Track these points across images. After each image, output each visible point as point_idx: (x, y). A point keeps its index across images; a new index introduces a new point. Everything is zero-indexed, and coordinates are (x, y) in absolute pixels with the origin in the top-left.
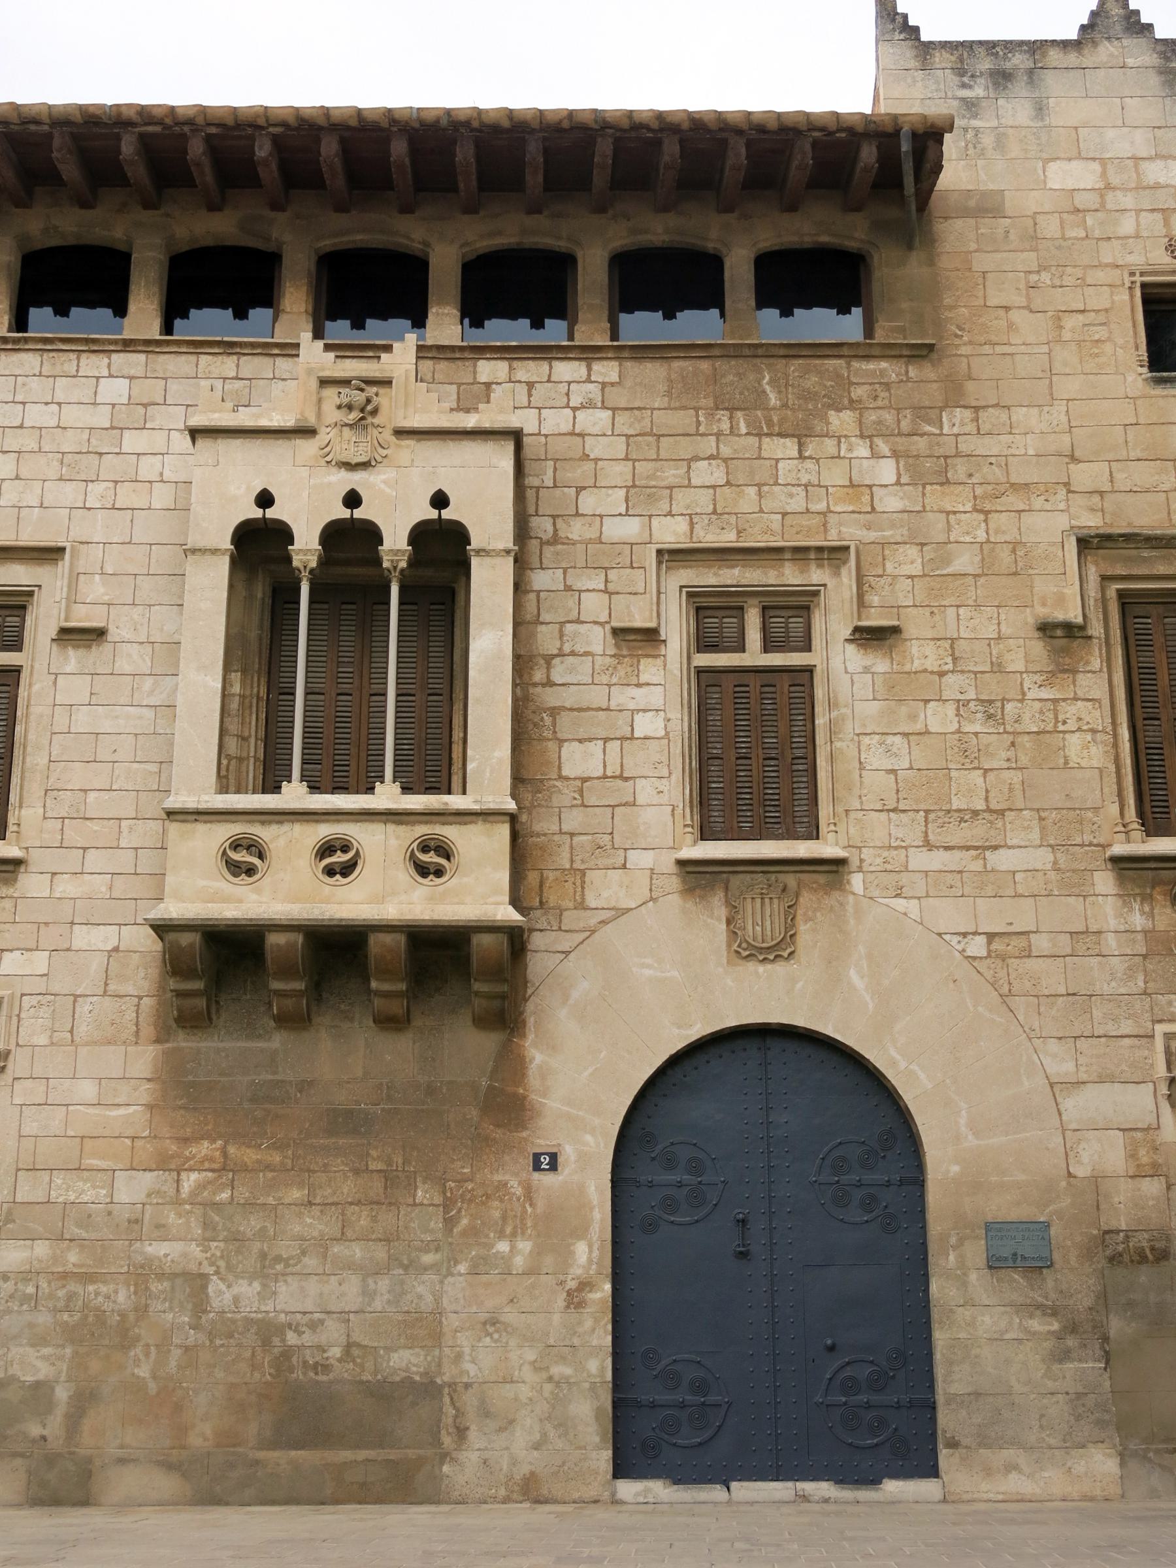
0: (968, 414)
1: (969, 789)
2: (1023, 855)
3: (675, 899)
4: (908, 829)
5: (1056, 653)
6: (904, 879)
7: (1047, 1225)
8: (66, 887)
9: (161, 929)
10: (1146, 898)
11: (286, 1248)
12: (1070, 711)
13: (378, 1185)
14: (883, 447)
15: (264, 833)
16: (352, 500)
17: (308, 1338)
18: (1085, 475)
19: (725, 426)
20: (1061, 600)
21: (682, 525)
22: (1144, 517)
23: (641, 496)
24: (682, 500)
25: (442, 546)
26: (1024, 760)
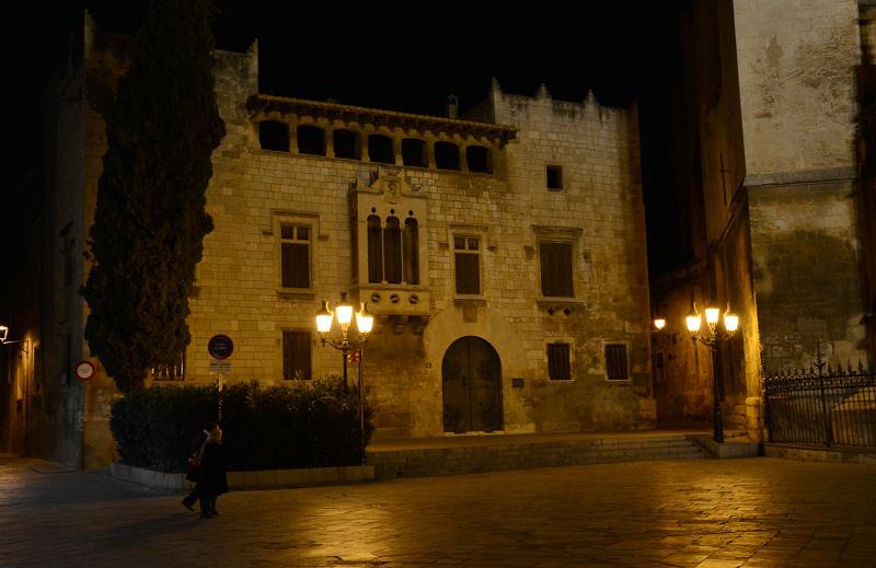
1: (510, 285)
2: (520, 300)
3: (452, 308)
5: (528, 254)
15: (380, 292)
16: (392, 211)
23: (444, 209)
24: (452, 211)
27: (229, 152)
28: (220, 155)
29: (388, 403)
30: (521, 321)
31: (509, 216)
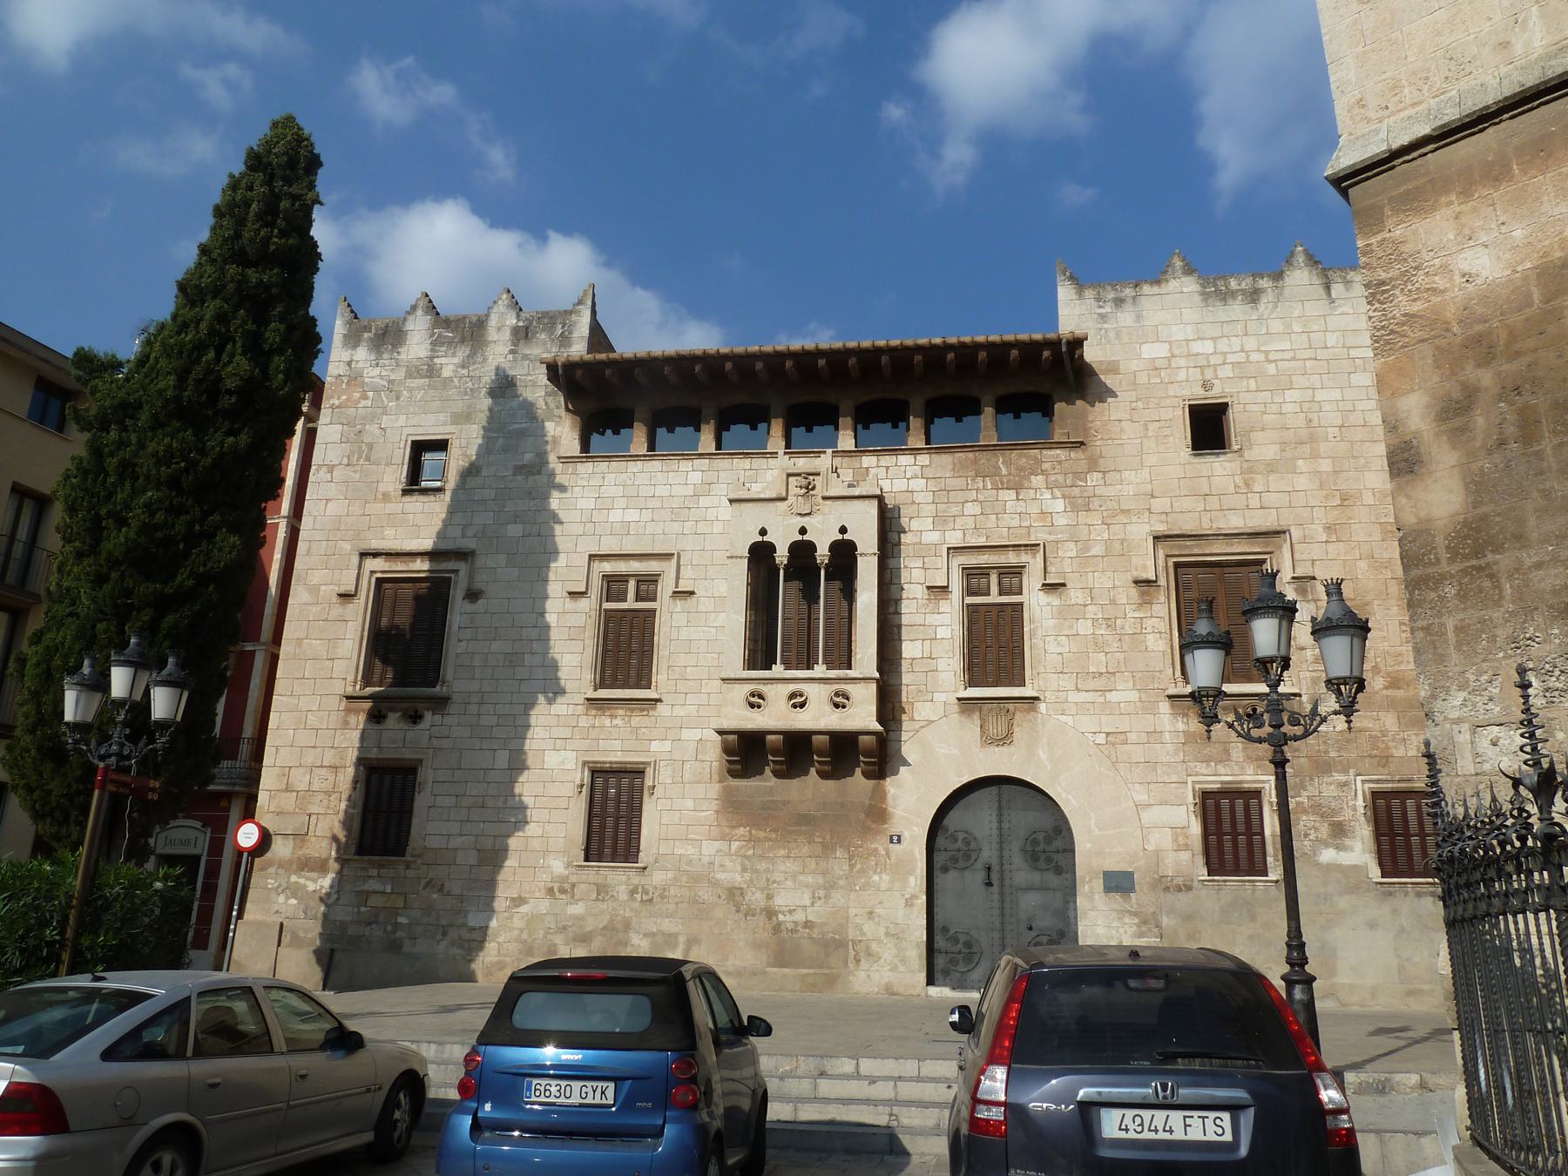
0: (1100, 475)
1: (1098, 662)
2: (1124, 694)
3: (956, 716)
4: (1066, 682)
5: (1142, 594)
6: (1066, 706)
7: (1131, 874)
8: (678, 711)
9: (721, 733)
10: (1185, 715)
11: (778, 876)
12: (1149, 623)
13: (819, 849)
14: (1057, 493)
15: (764, 688)
17: (788, 918)
18: (1159, 504)
19: (981, 485)
20: (1145, 567)
21: (959, 534)
22: (1189, 526)
23: (940, 520)
24: (960, 522)
25: (844, 552)
26: (1125, 648)
27: (523, 466)
28: (510, 472)
29: (800, 916)
30: (1125, 742)
31: (1095, 518)
